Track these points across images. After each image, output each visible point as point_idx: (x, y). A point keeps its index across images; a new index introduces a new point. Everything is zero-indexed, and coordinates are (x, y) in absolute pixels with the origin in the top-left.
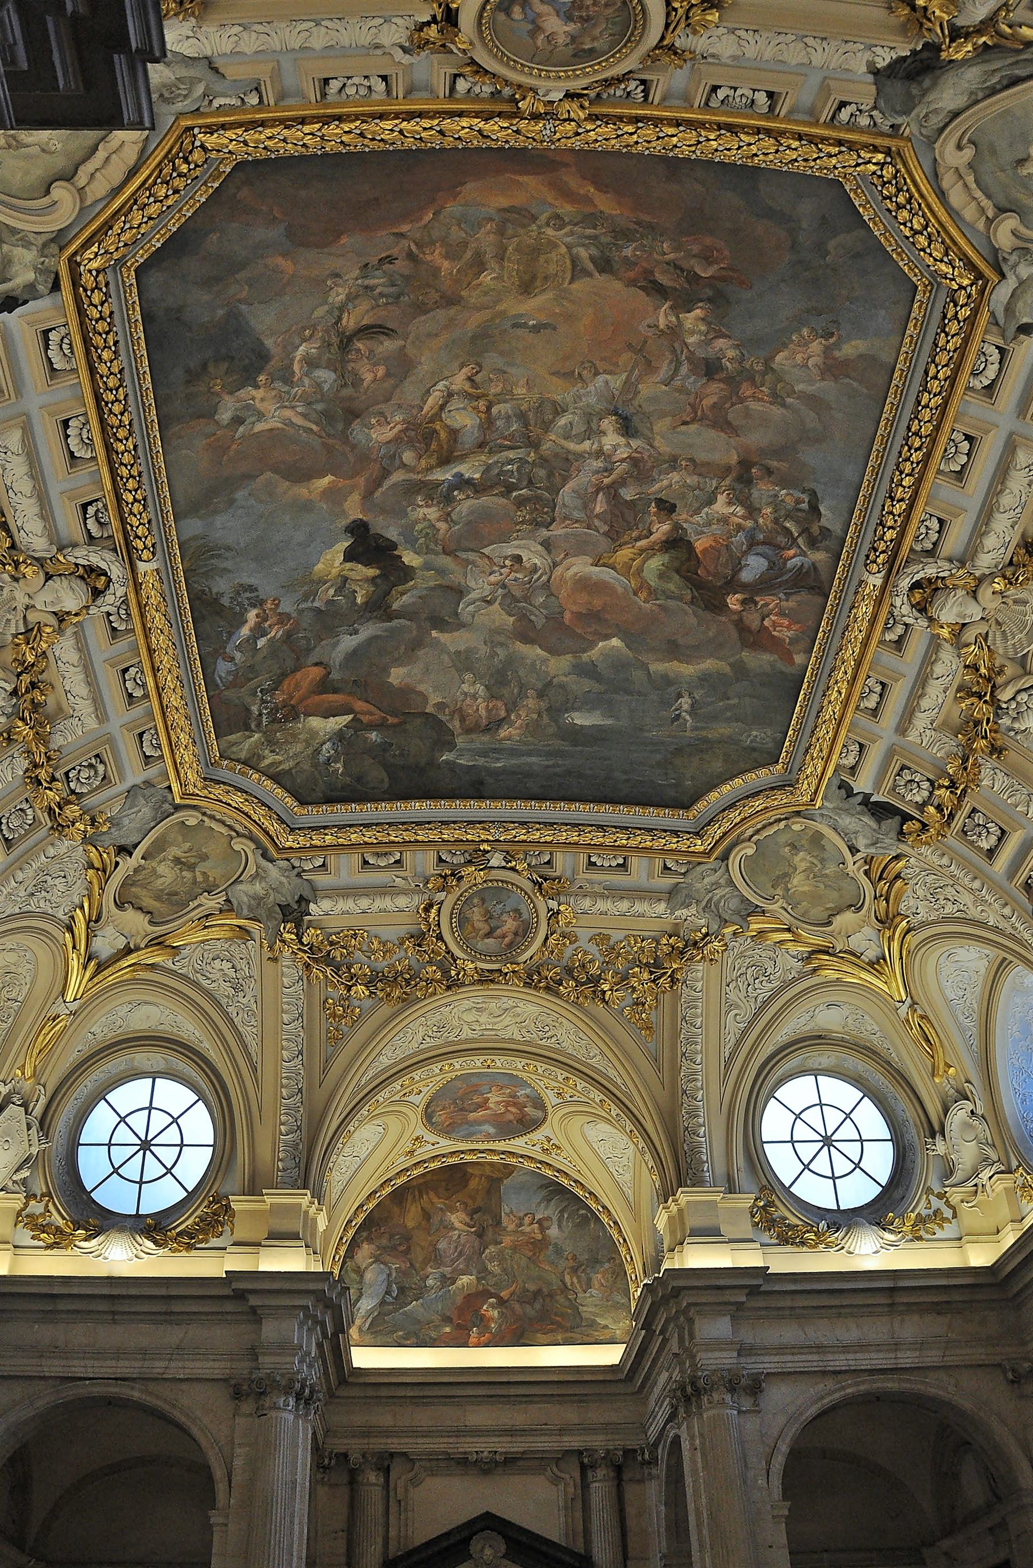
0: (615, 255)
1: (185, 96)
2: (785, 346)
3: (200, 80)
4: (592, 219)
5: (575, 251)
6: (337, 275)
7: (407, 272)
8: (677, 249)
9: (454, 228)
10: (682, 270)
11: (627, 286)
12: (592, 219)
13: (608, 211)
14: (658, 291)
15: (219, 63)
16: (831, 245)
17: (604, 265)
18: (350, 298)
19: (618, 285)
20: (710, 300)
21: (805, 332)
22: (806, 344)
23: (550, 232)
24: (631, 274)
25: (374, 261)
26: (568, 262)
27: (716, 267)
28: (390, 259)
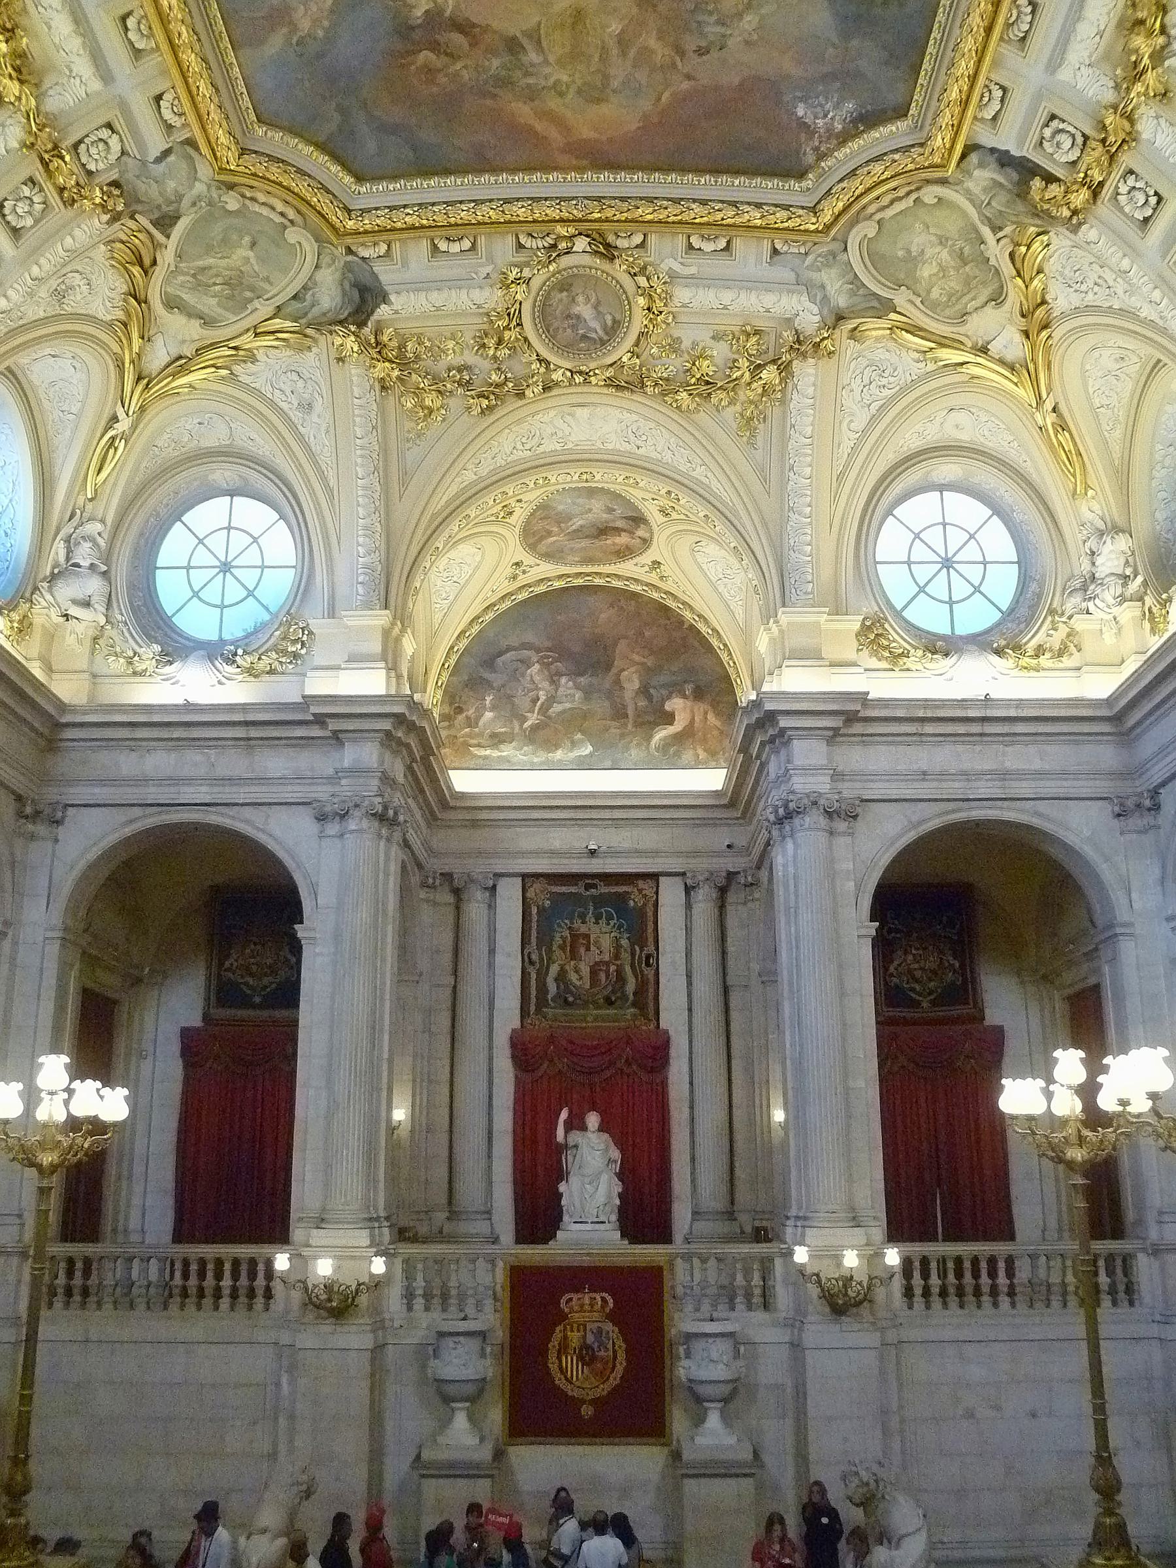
0: (507, 58)
1: (819, 256)
2: (332, 11)
3: (807, 268)
4: (532, 95)
5: (541, 59)
6: (747, 43)
7: (687, 37)
8: (457, 74)
9: (644, 82)
10: (447, 54)
11: (488, 25)
12: (532, 95)
13: (520, 105)
14: (463, 27)
15: (793, 275)
16: (337, 117)
17: (513, 46)
18: (740, 15)
19: (495, 24)
20: (413, 28)
21: (320, 33)
22: (316, 22)
23: (565, 78)
24: (488, 38)
25: (714, 54)
26: (544, 44)
27: (419, 64)
28: (701, 52)
